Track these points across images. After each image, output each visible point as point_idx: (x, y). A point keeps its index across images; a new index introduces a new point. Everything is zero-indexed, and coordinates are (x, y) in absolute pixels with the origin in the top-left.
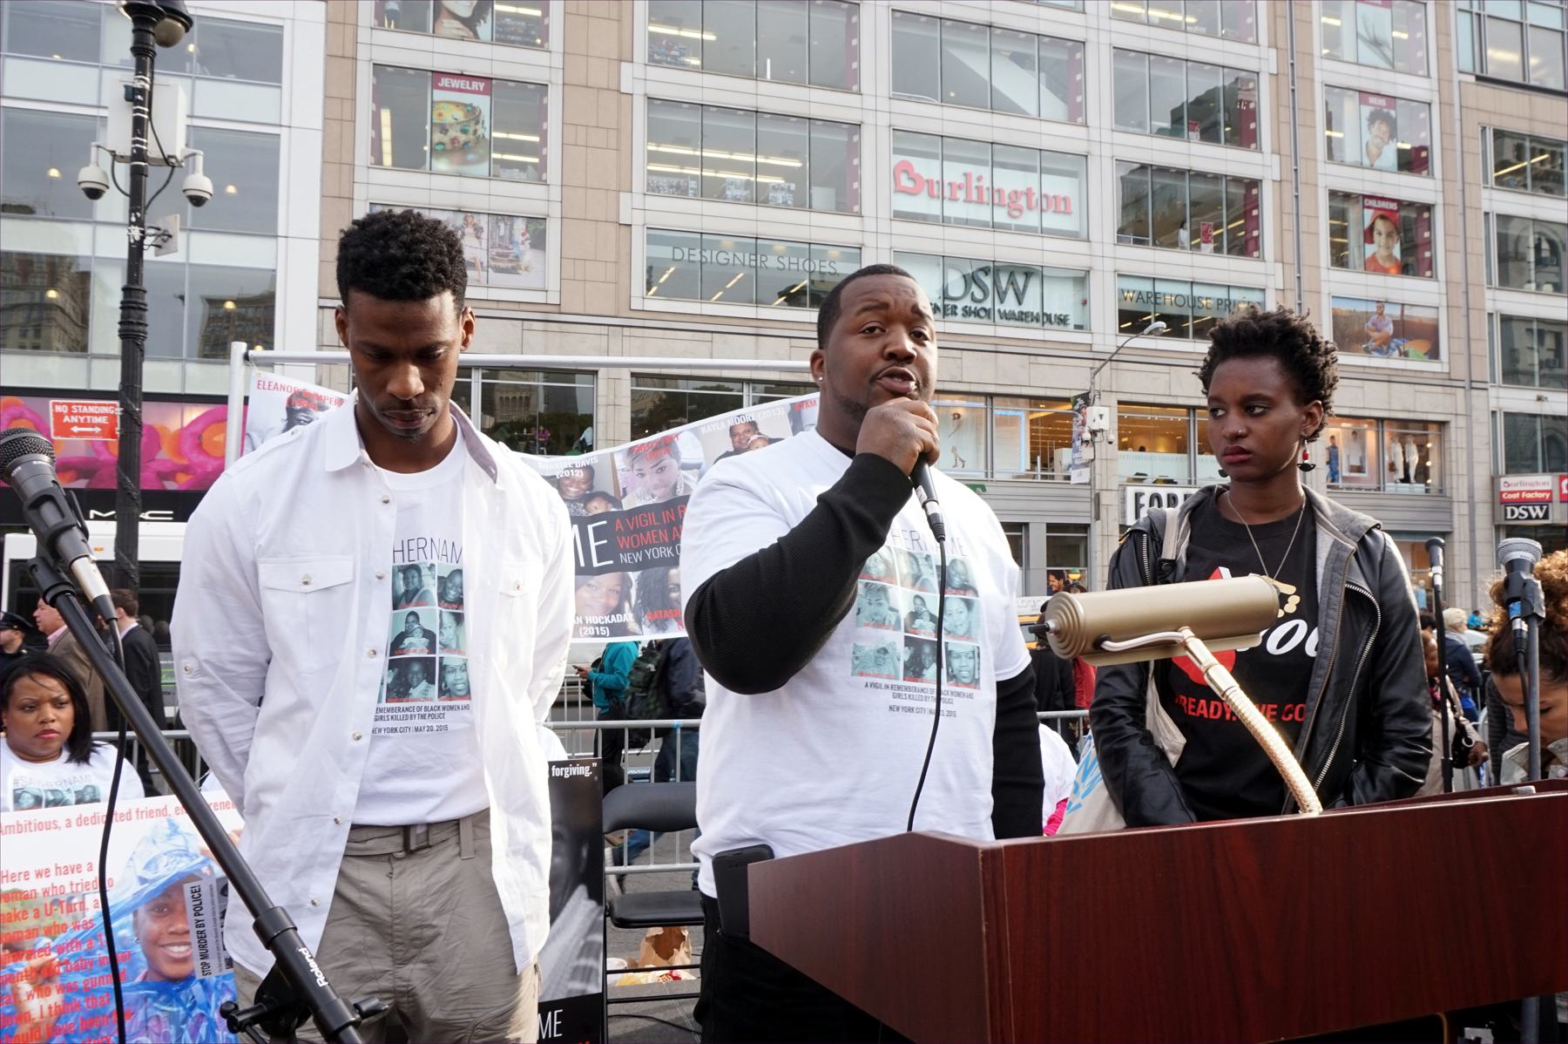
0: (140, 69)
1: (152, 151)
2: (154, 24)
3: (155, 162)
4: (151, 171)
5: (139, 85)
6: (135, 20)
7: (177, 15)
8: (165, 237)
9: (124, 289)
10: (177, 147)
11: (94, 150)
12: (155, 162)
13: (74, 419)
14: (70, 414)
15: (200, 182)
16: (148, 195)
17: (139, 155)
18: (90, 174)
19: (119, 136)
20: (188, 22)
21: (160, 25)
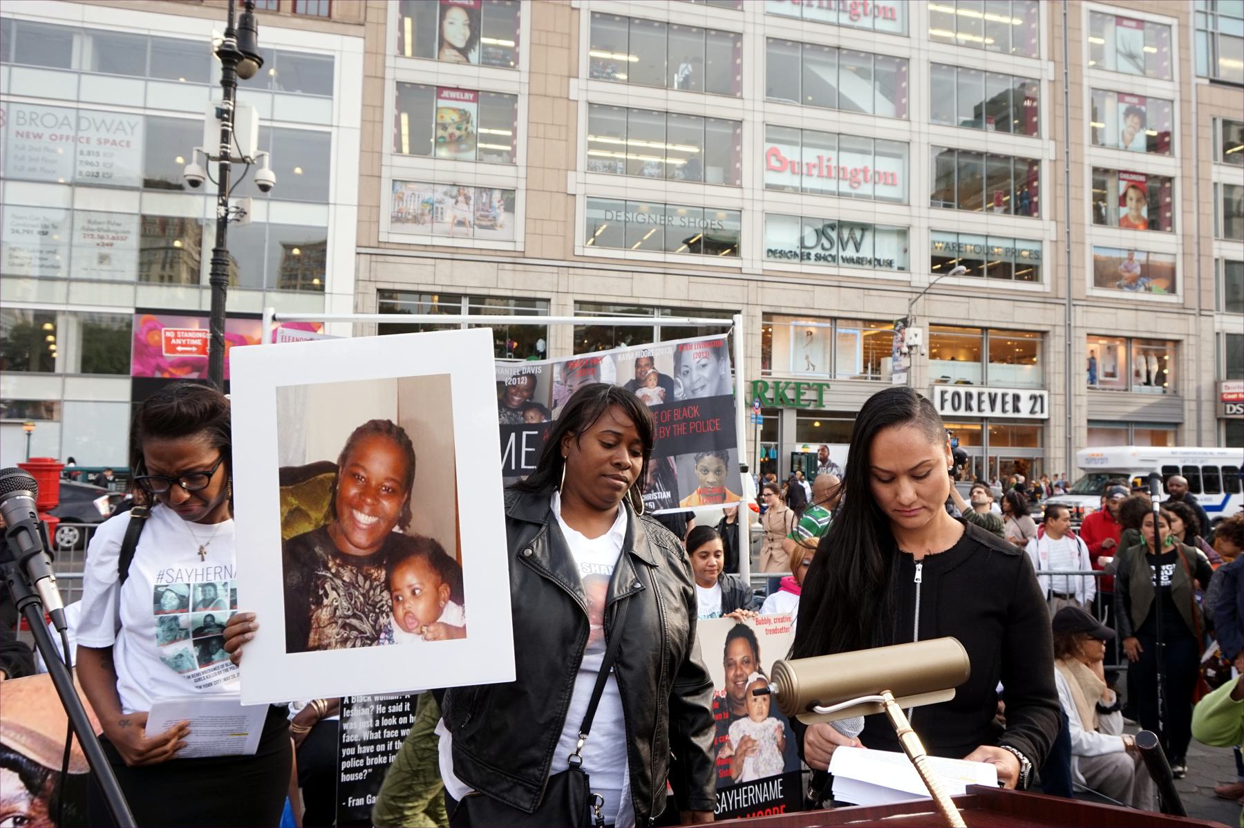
0: (227, 95)
1: (234, 153)
2: (236, 64)
3: (235, 161)
4: (234, 166)
5: (225, 107)
6: (224, 62)
7: (252, 56)
8: (242, 213)
9: (215, 251)
10: (252, 151)
11: (195, 153)
12: (235, 161)
13: (179, 341)
14: (176, 338)
15: (267, 175)
16: (230, 184)
17: (225, 156)
18: (193, 170)
19: (212, 145)
20: (260, 62)
21: (241, 64)
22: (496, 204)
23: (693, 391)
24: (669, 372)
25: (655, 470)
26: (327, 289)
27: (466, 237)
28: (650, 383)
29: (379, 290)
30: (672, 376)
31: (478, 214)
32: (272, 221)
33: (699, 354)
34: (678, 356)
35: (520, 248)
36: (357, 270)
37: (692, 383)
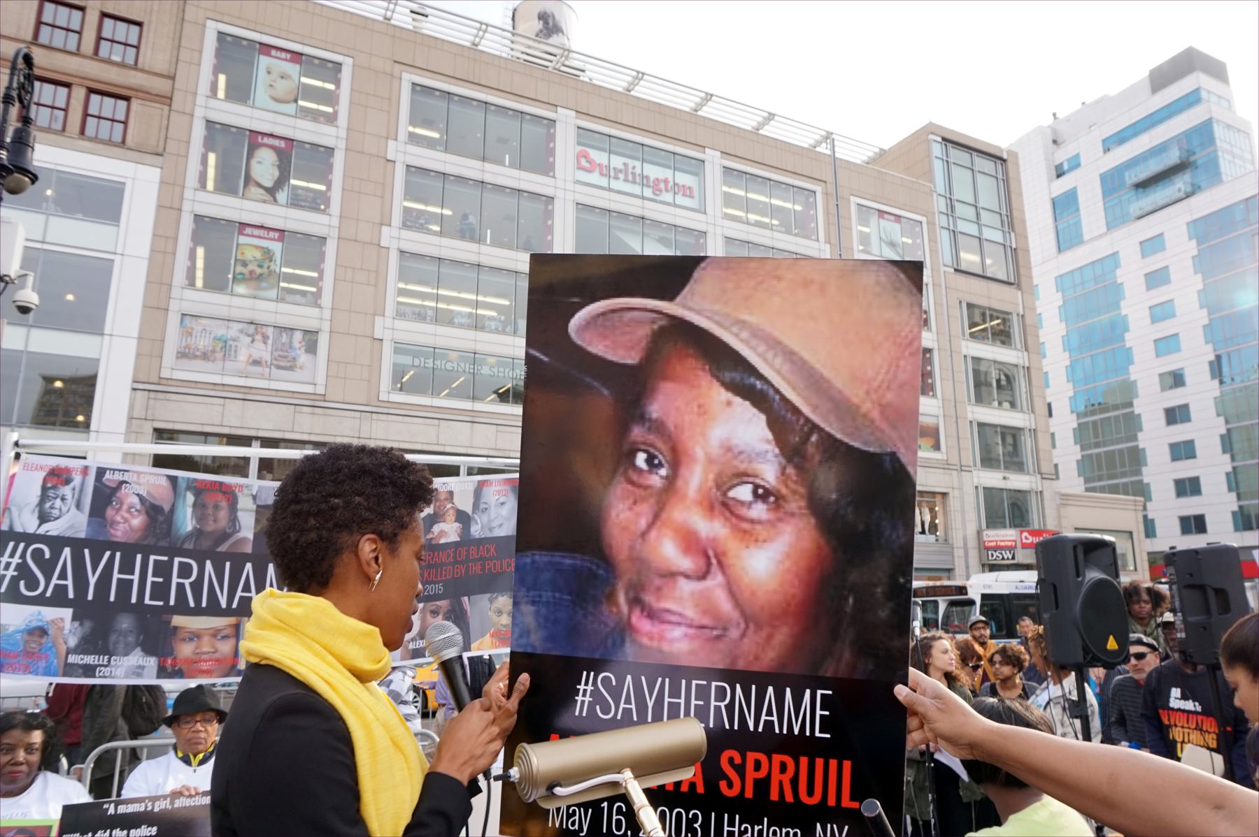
22: (296, 344)
23: (491, 529)
24: (467, 507)
25: (449, 611)
26: (93, 427)
27: (262, 377)
28: (448, 518)
29: (156, 430)
30: (469, 510)
31: (276, 354)
32: (31, 349)
33: (499, 492)
34: (478, 493)
35: (321, 390)
36: (131, 407)
37: (490, 521)
